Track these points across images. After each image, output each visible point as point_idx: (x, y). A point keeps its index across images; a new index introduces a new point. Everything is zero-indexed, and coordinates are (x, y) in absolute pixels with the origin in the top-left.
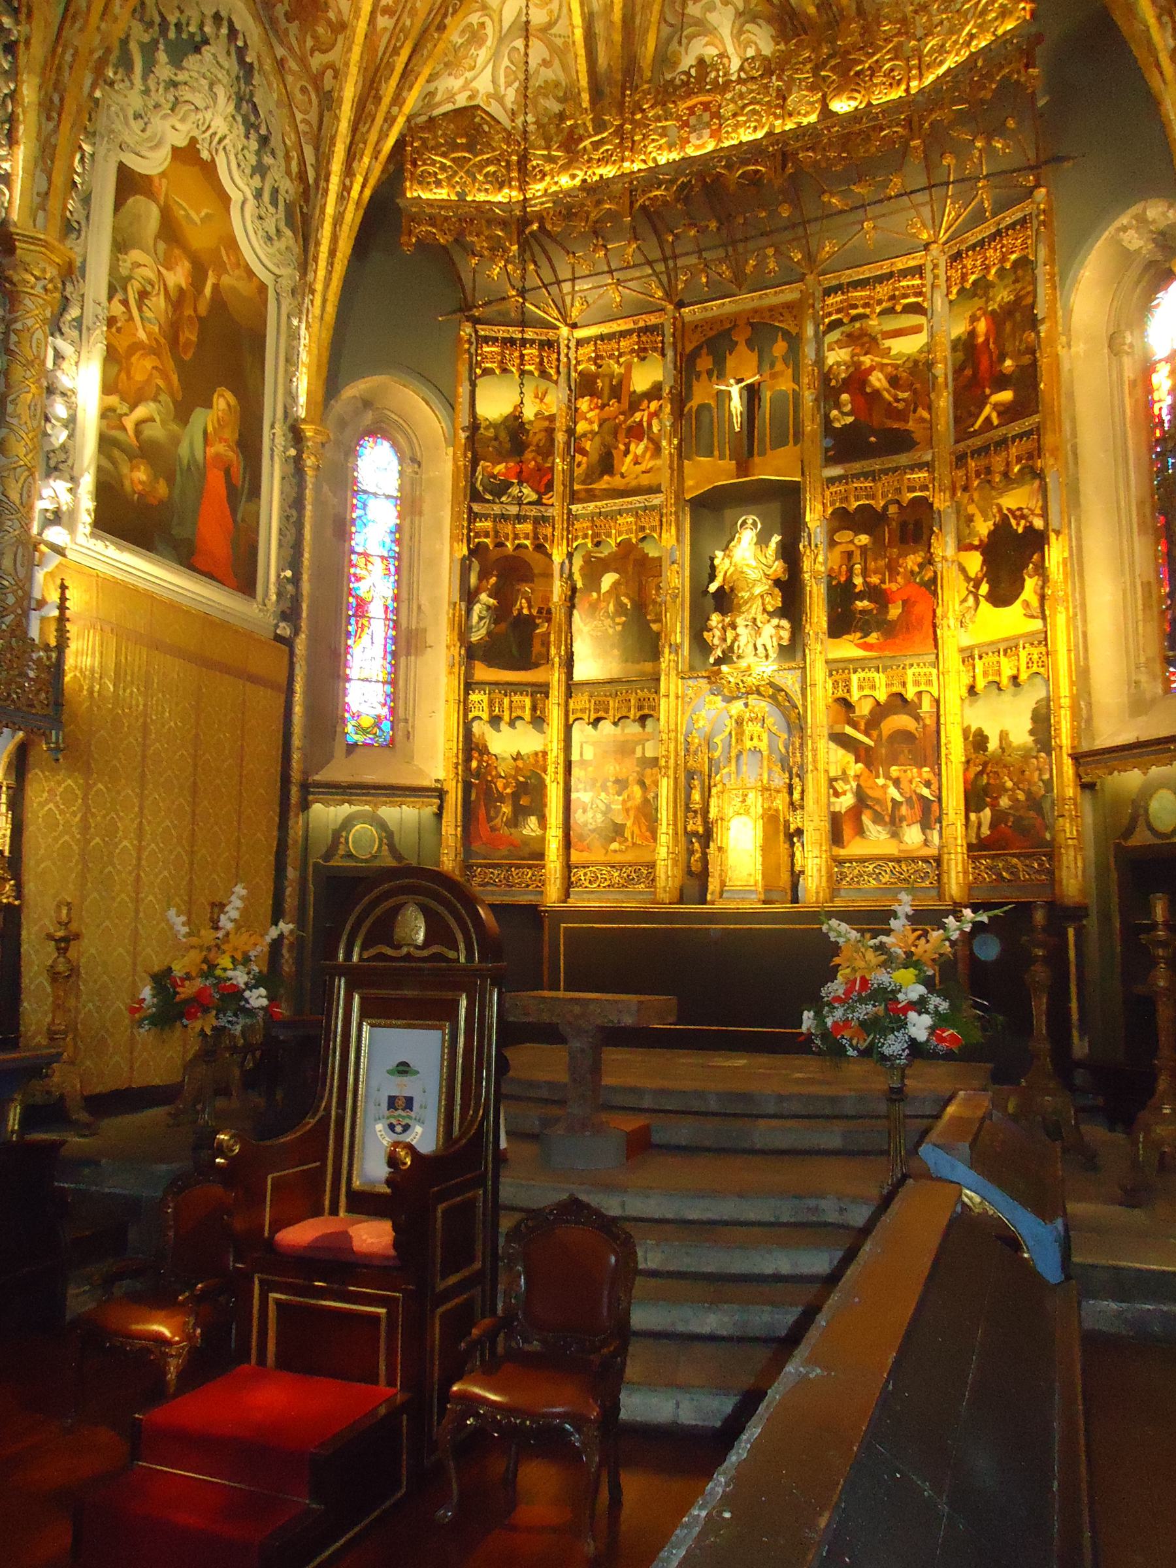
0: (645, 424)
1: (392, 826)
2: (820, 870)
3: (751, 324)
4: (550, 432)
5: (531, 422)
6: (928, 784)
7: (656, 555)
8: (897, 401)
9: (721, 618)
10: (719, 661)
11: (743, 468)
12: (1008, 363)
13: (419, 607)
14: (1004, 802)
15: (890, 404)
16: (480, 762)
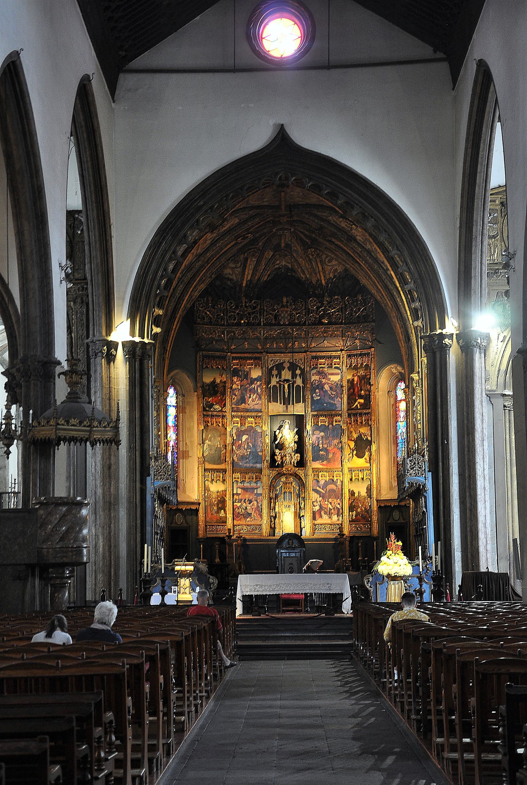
4: (224, 387)
12: (363, 392)
14: (359, 510)
16: (208, 494)
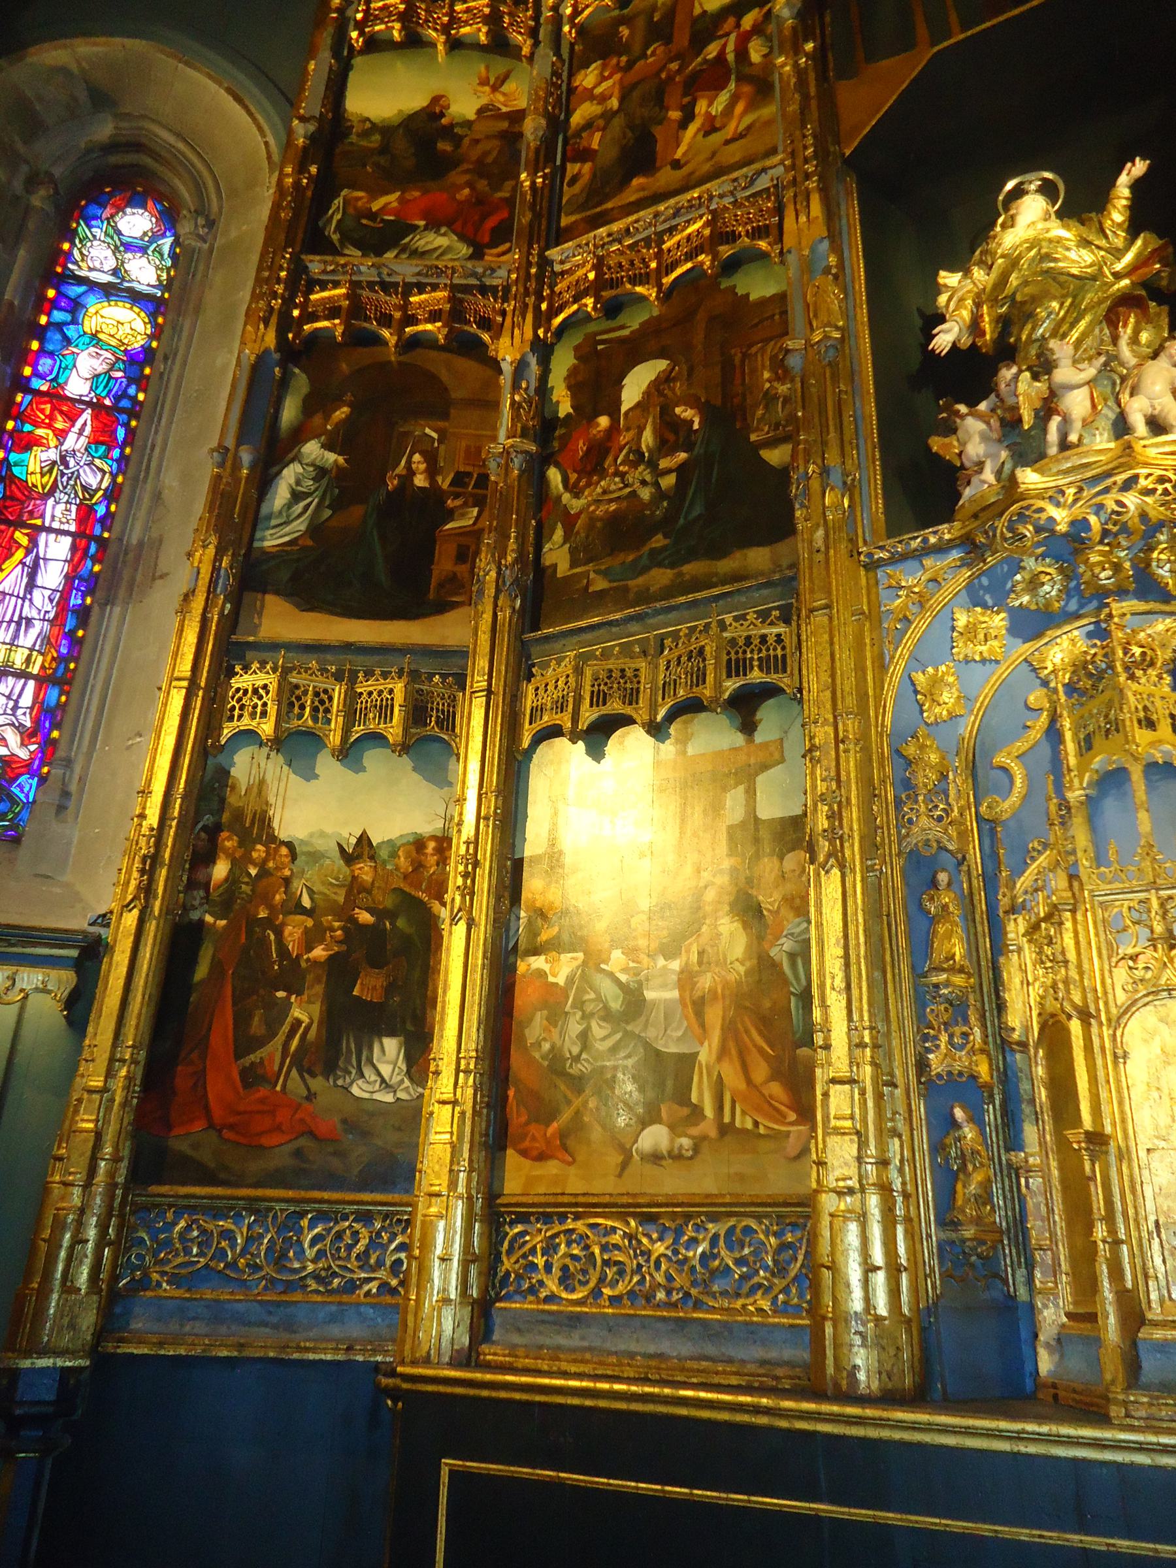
0: (731, 57)
4: (512, 137)
5: (468, 124)
13: (157, 497)
16: (238, 865)
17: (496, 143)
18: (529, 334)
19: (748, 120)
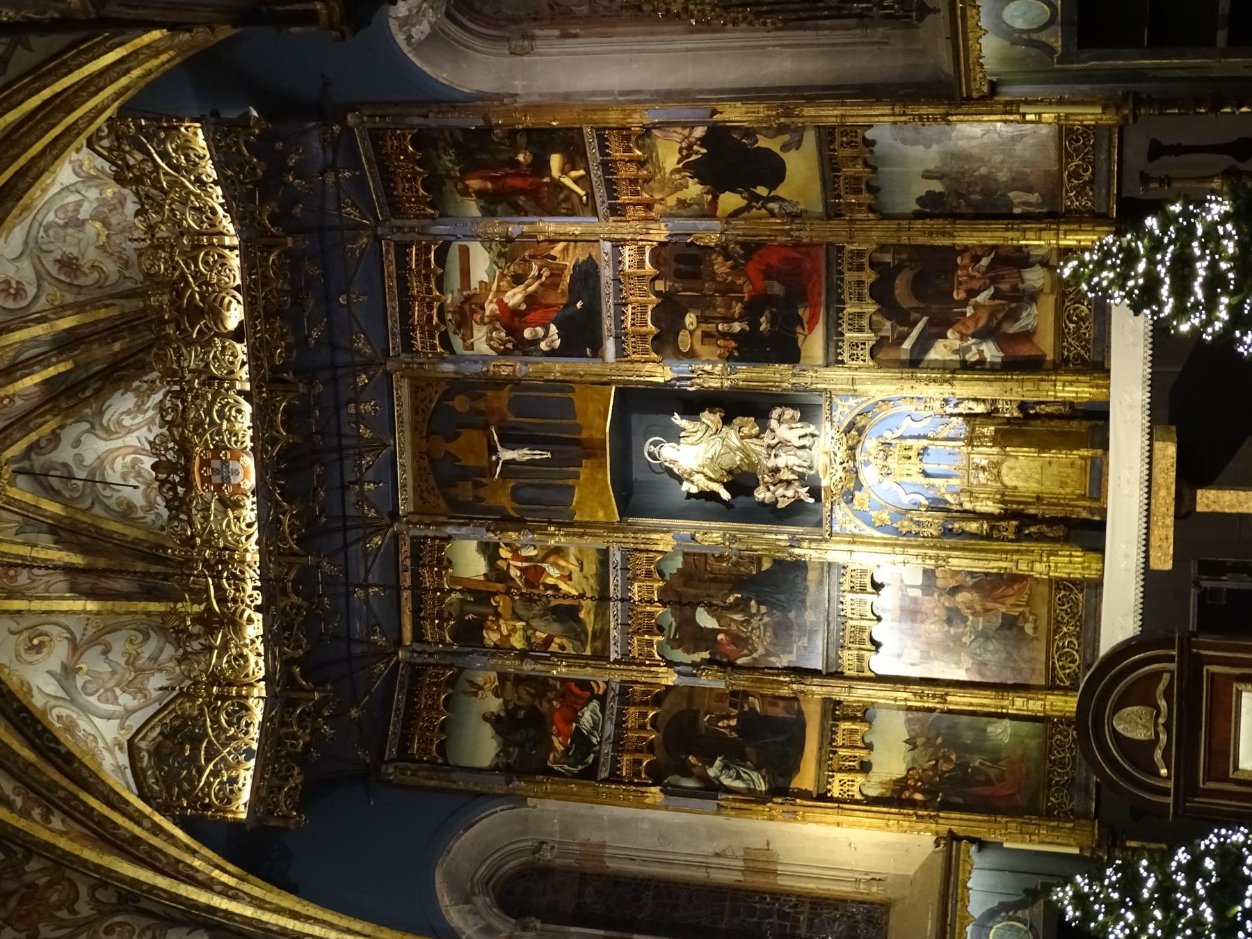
0: (525, 564)
1: (993, 903)
2: (1071, 383)
3: (427, 437)
4: (519, 680)
5: (506, 703)
6: (976, 259)
7: (680, 559)
8: (540, 276)
9: (762, 488)
10: (815, 492)
11: (591, 450)
12: (521, 157)
13: (717, 855)
15: (542, 284)
16: (917, 790)
17: (521, 688)
18: (665, 669)
19: (572, 559)
